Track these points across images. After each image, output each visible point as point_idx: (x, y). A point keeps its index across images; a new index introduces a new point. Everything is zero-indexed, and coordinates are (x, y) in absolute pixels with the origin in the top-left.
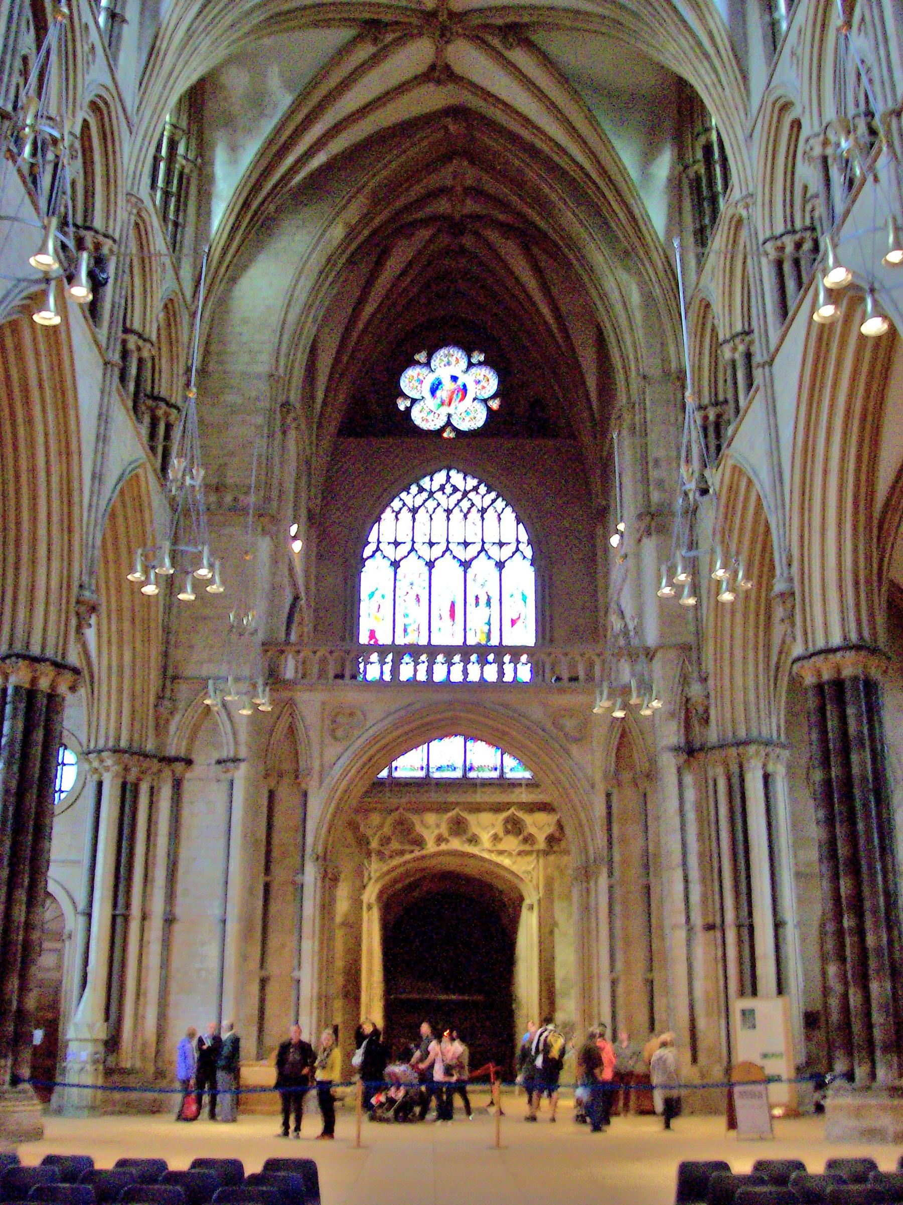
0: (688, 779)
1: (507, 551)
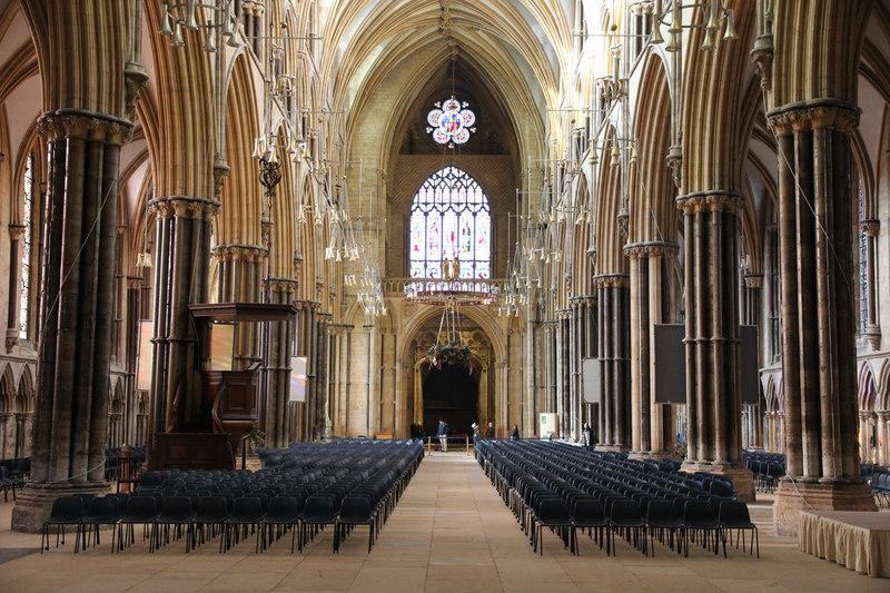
0: (537, 333)
1: (478, 207)
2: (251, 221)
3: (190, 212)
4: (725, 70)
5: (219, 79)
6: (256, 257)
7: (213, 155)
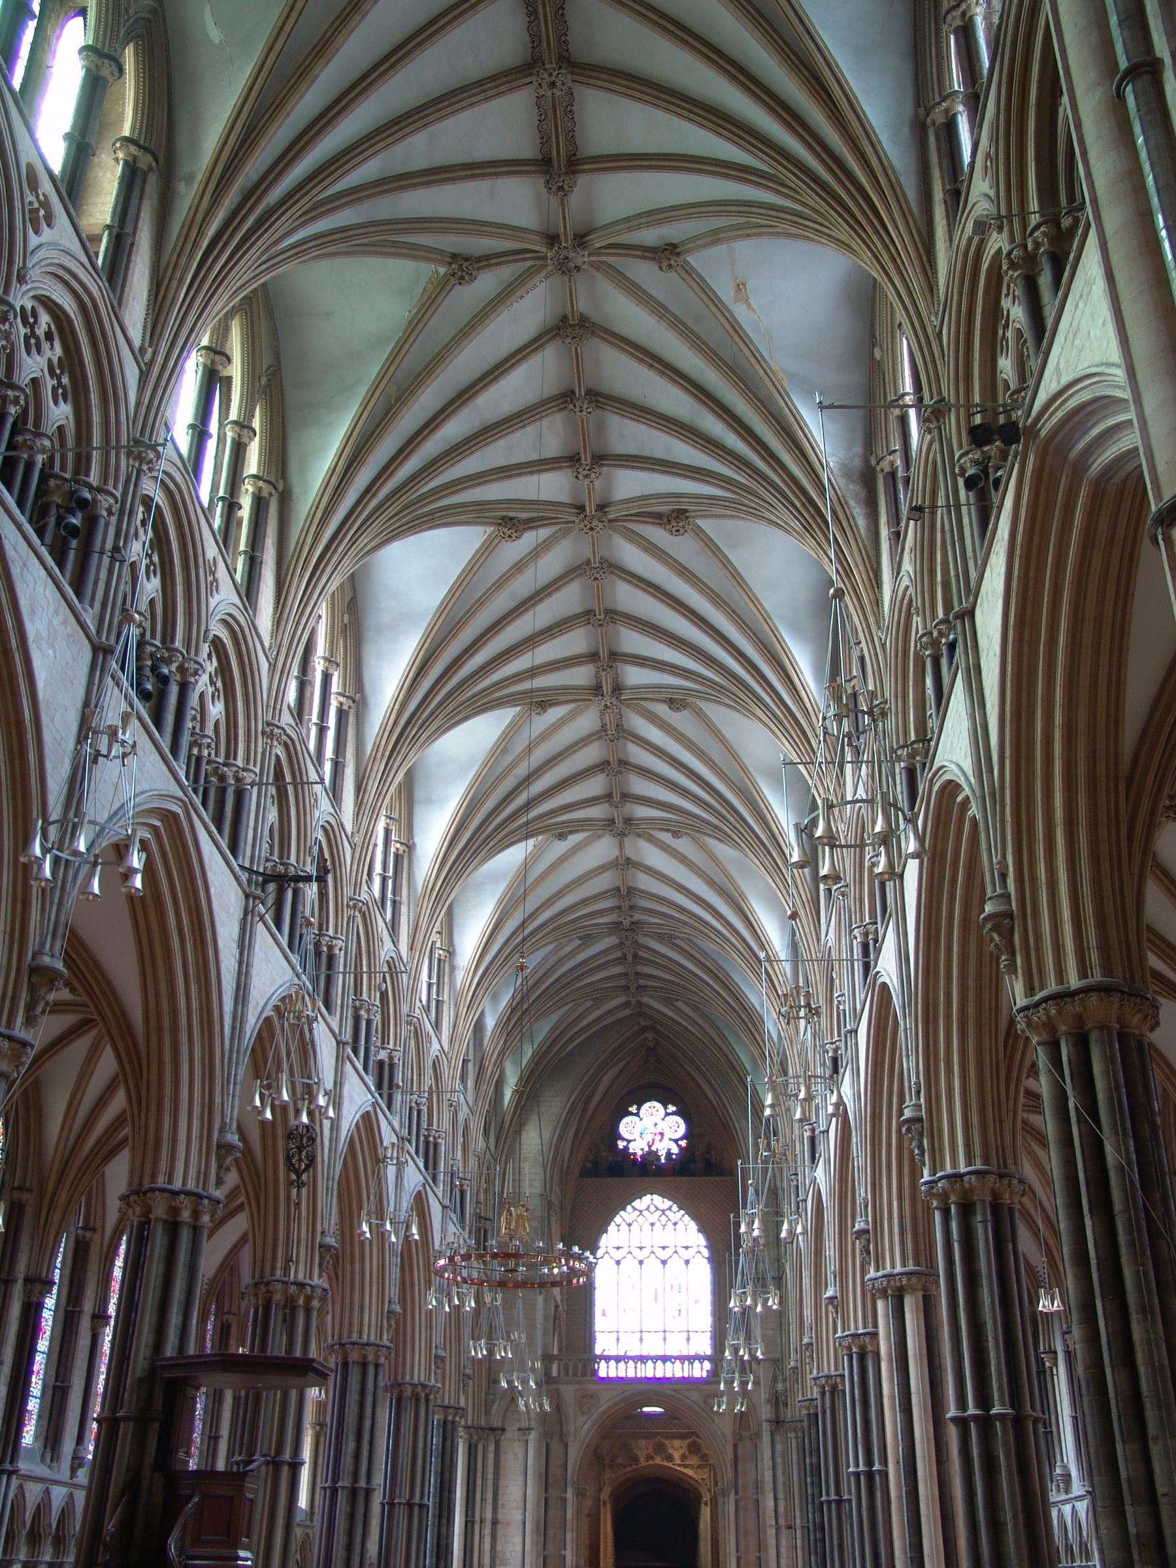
0: (778, 1438)
1: (691, 1252)
2: (303, 1243)
3: (175, 1211)
4: (971, 984)
5: (239, 1018)
6: (308, 1299)
7: (217, 1125)
